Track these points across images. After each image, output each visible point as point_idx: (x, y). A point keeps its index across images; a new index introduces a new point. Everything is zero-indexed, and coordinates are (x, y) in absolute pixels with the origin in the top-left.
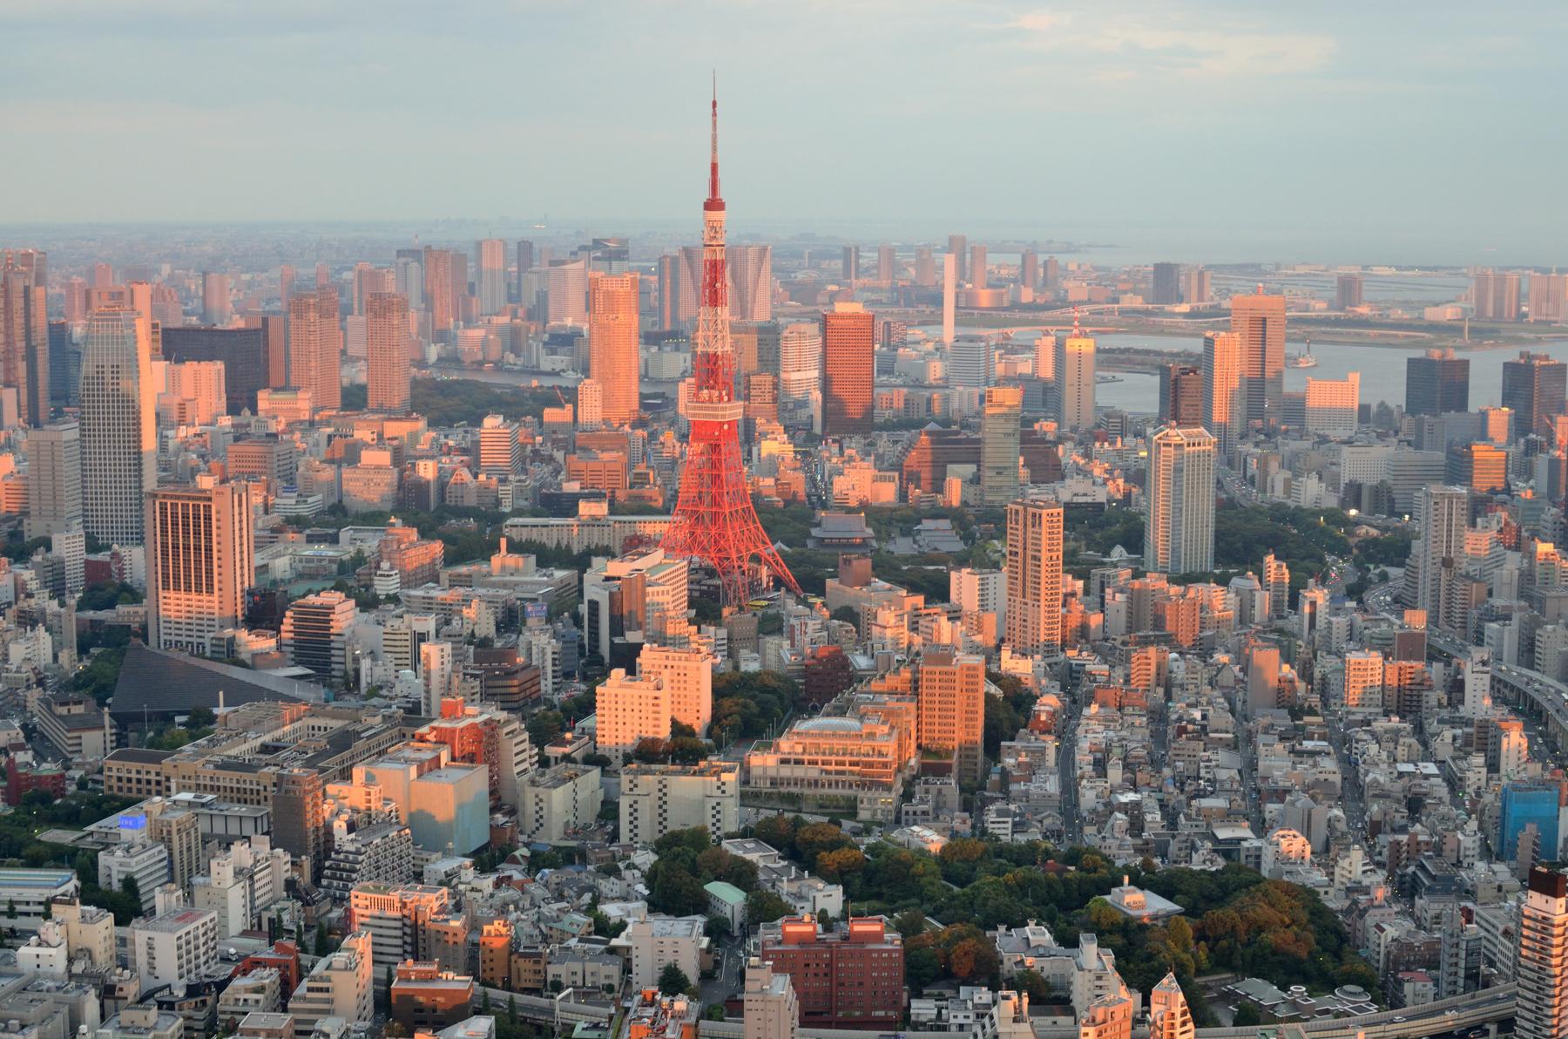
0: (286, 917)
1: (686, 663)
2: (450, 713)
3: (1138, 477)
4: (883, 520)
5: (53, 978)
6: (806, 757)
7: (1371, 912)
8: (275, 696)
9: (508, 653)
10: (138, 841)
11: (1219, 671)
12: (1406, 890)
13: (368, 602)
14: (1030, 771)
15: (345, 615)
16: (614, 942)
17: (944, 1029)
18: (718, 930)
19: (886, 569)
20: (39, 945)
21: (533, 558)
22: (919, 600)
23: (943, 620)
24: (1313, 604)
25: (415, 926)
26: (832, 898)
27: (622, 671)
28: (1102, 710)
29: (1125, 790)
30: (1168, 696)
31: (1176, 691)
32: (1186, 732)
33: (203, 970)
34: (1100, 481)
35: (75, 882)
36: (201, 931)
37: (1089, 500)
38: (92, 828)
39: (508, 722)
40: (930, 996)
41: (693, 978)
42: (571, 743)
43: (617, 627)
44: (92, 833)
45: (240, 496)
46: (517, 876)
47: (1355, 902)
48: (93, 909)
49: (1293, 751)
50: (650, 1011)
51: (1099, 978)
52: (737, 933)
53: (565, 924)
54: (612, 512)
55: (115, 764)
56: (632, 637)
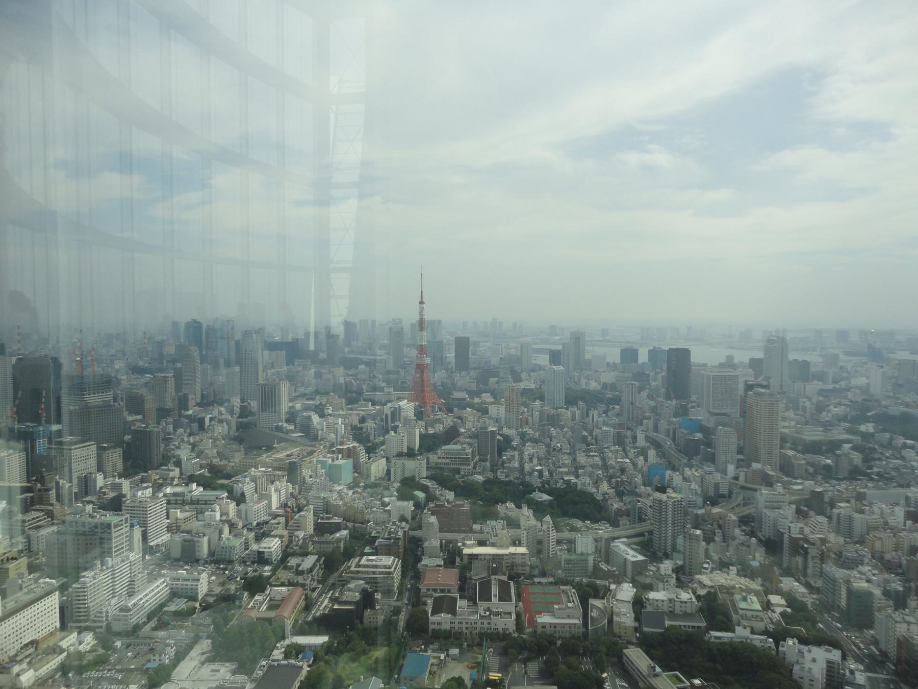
0: (289, 503)
2: (342, 443)
3: (543, 382)
4: (472, 394)
5: (215, 521)
6: (446, 456)
8: (293, 441)
12: (620, 495)
13: (322, 415)
15: (315, 419)
16: (386, 508)
17: (483, 533)
18: (417, 505)
19: (471, 406)
20: (212, 512)
22: (480, 414)
23: (486, 419)
25: (327, 504)
26: (450, 495)
27: (393, 432)
28: (531, 444)
30: (551, 441)
33: (262, 519)
35: (226, 494)
36: (262, 506)
37: (529, 388)
38: (234, 479)
39: (359, 447)
40: (478, 523)
41: (409, 518)
43: (393, 422)
44: (233, 481)
46: (359, 491)
47: (605, 497)
48: (229, 500)
49: (587, 455)
50: (394, 527)
51: (528, 518)
52: (423, 506)
53: (372, 504)
56: (397, 423)
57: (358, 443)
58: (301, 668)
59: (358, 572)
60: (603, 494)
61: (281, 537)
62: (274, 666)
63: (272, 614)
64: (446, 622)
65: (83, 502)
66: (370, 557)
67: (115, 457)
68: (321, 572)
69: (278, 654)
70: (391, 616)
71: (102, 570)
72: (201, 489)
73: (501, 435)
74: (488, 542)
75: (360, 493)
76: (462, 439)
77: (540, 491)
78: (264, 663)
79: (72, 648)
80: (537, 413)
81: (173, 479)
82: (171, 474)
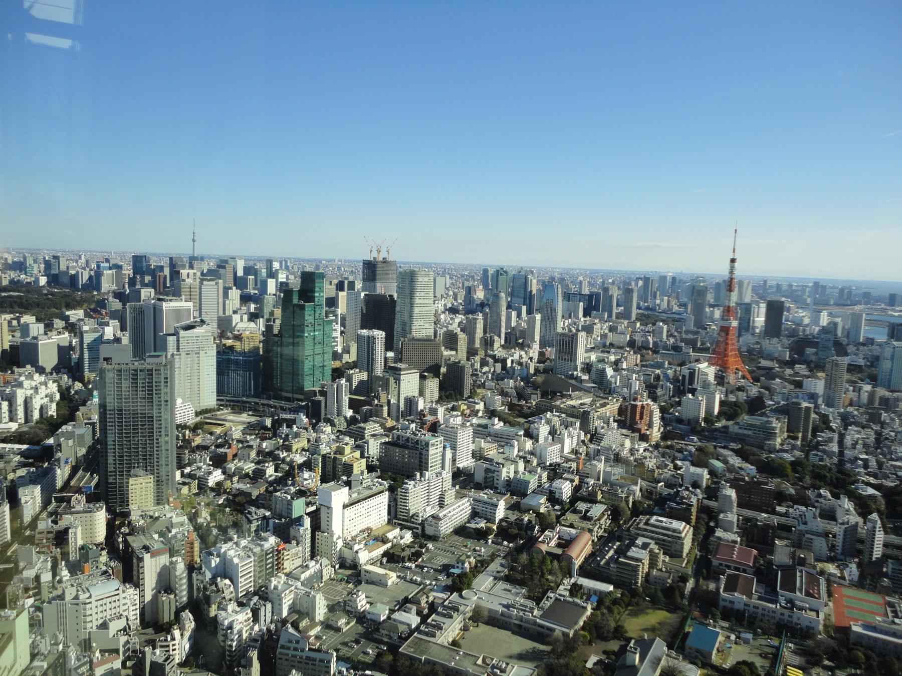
15: (610, 372)
16: (679, 472)
18: (711, 473)
22: (792, 387)
27: (690, 395)
30: (882, 427)
31: (885, 426)
33: (555, 461)
56: (694, 387)
57: (653, 401)
58: (585, 608)
59: (646, 530)
61: (572, 481)
62: (560, 600)
63: (559, 551)
64: (739, 603)
65: (408, 420)
66: (660, 518)
67: (433, 385)
68: (609, 522)
69: (563, 590)
70: (678, 581)
71: (420, 481)
72: (502, 424)
73: (816, 413)
74: (793, 529)
75: (651, 452)
78: (552, 595)
79: (395, 540)
80: (866, 394)
81: (478, 411)
82: (477, 407)
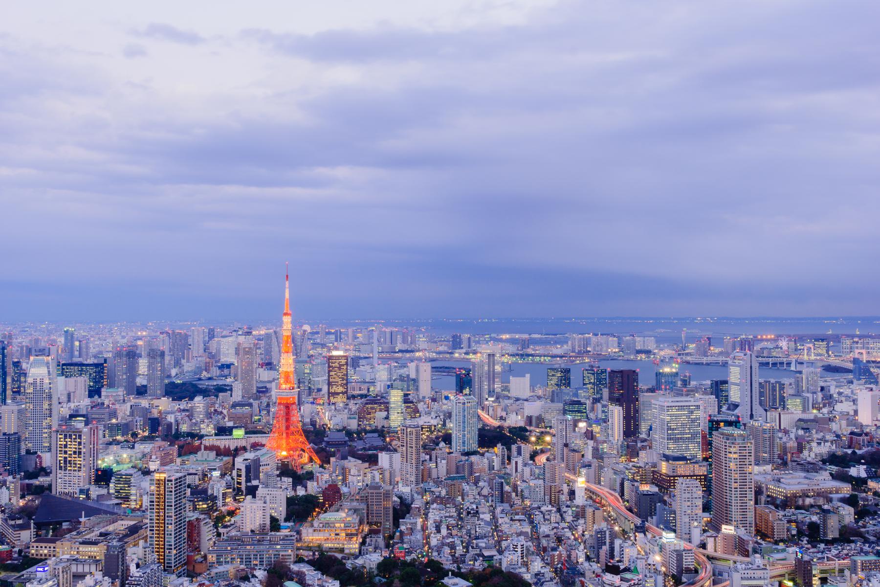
1: (276, 493)
7: (545, 583)
8: (106, 512)
9: (205, 491)
10: (44, 577)
11: (482, 489)
14: (412, 531)
21: (215, 452)
22: (367, 465)
24: (516, 463)
28: (438, 506)
29: (448, 537)
32: (470, 514)
34: (434, 417)
38: (24, 572)
39: (204, 519)
42: (229, 526)
43: (248, 480)
44: (23, 575)
45: (94, 431)
47: (539, 580)
49: (512, 520)
54: (246, 433)
55: (35, 545)
56: (255, 483)
60: (537, 575)
76: (347, 504)
77: (456, 574)
